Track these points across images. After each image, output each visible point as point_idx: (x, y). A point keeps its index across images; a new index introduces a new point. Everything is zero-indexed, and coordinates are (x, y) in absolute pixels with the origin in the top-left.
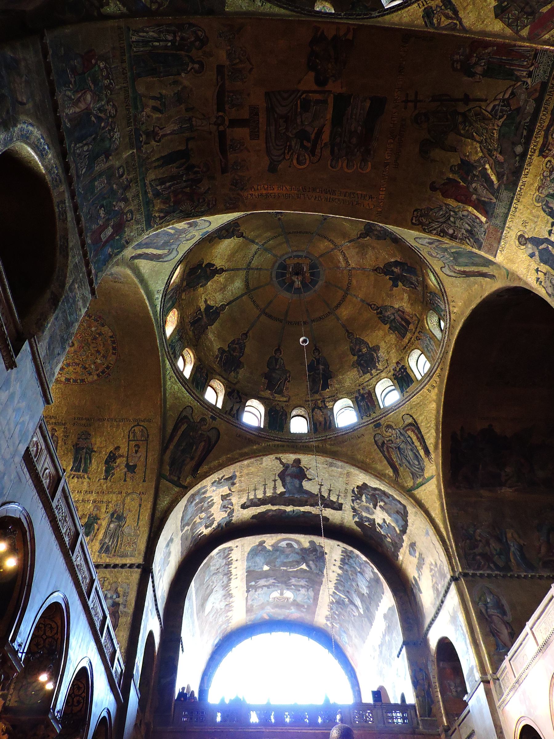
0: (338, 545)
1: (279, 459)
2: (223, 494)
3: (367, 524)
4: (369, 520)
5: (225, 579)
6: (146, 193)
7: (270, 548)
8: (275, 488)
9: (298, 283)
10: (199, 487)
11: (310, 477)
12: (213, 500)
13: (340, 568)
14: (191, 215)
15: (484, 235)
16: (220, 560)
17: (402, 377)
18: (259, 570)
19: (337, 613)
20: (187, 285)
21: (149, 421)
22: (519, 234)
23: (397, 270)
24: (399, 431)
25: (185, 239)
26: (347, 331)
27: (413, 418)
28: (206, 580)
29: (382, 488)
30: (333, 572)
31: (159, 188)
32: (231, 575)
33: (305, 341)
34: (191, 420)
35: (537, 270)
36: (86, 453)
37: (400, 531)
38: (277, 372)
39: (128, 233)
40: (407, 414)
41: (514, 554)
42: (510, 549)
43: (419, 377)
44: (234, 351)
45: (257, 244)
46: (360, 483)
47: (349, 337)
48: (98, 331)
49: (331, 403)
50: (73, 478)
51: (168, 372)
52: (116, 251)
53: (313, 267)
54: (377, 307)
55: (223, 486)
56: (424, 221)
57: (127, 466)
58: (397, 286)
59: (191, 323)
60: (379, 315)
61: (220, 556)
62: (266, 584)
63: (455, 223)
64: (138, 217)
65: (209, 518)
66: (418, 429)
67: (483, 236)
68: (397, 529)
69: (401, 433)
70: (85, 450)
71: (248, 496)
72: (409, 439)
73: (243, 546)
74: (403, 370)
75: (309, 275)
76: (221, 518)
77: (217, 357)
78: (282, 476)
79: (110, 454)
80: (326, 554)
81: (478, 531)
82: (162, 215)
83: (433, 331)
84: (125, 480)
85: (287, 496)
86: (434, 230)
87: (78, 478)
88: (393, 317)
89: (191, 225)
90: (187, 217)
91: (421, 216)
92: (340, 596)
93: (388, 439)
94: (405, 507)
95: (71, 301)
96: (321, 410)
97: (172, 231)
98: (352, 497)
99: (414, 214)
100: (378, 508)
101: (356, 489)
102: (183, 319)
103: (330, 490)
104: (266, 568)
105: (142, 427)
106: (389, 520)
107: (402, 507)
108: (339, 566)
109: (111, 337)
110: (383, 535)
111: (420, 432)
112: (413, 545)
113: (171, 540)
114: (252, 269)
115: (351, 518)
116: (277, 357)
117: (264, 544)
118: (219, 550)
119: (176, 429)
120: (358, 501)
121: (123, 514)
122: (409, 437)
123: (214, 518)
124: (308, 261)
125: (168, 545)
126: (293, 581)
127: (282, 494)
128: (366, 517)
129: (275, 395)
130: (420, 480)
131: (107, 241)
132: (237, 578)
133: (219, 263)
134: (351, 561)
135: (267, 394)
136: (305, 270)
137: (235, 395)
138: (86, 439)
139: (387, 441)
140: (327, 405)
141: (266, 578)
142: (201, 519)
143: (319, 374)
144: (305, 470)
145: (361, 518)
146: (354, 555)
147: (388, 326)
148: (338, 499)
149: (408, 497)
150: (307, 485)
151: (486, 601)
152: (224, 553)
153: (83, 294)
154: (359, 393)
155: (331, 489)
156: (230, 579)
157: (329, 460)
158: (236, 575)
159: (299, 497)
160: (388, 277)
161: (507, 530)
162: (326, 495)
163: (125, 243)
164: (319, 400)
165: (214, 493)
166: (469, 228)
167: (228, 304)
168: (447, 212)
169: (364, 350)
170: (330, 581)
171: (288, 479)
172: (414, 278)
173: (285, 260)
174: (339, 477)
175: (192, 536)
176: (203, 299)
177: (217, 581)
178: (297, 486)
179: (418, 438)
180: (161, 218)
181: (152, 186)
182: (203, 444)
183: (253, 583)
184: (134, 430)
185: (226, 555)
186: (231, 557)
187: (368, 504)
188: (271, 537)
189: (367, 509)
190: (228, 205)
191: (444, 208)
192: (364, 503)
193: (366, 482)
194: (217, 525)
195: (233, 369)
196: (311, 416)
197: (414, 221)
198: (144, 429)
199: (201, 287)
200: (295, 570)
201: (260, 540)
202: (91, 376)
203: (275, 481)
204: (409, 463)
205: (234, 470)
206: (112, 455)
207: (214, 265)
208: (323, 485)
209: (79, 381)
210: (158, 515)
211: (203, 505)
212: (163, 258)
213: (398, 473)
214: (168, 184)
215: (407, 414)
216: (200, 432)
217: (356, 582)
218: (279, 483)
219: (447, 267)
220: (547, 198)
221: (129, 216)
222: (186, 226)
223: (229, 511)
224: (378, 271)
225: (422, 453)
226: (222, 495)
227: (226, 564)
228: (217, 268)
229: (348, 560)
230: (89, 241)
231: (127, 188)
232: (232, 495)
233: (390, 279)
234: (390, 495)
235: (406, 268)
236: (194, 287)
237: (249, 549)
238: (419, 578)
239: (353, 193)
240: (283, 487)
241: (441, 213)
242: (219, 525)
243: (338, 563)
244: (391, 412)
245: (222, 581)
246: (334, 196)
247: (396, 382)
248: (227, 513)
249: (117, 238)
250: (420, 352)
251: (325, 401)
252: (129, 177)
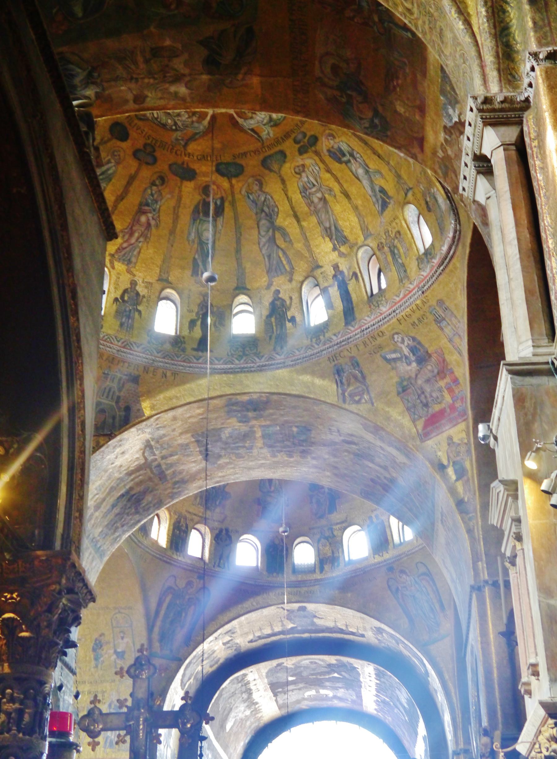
5: (245, 696)
21: (130, 608)
33: (284, 532)
57: (116, 652)
66: (433, 580)
72: (424, 589)
111: (435, 584)
215: (421, 563)
216: (187, 597)
225: (437, 606)
237: (266, 671)
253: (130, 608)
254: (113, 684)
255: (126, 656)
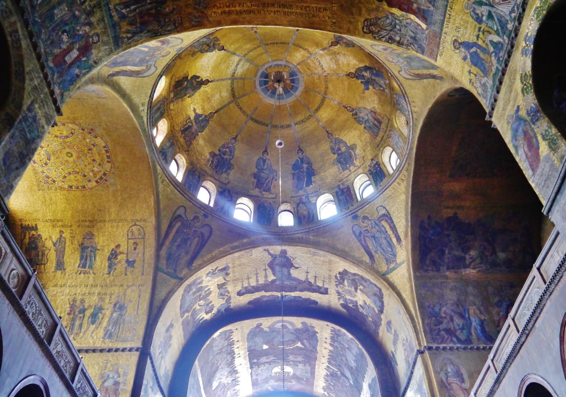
0: (327, 325)
1: (267, 251)
2: (219, 283)
3: (351, 305)
4: (352, 302)
5: (229, 358)
6: (111, 16)
7: (267, 330)
8: (266, 276)
9: (280, 90)
10: (194, 278)
11: (296, 266)
12: (209, 289)
13: (331, 345)
14: (159, 34)
15: (426, 41)
16: (223, 342)
17: (376, 172)
18: (260, 349)
19: (332, 384)
20: (174, 97)
21: (145, 221)
22: (454, 39)
23: (367, 74)
24: (375, 221)
25: (160, 56)
26: (327, 132)
27: (386, 210)
28: (210, 359)
29: (360, 273)
30: (325, 348)
31: (124, 11)
32: (235, 354)
33: (280, 144)
34: (186, 219)
35: (470, 72)
36: (91, 251)
37: (378, 311)
38: (265, 171)
39: (95, 54)
40: (381, 206)
41: (476, 329)
42: (471, 324)
43: (391, 172)
44: (224, 154)
45: (239, 56)
46: (341, 270)
47: (329, 137)
48: (92, 142)
49: (315, 198)
50: (80, 274)
51: (160, 176)
52: (84, 71)
53: (292, 74)
54: (352, 109)
55: (218, 276)
56: (374, 29)
57: (127, 261)
58: (368, 89)
59: (181, 131)
60: (355, 117)
61: (222, 338)
62: (267, 361)
63: (400, 30)
64: (105, 39)
65: (208, 305)
66: (391, 219)
67: (425, 41)
68: (376, 309)
69: (375, 223)
70: (89, 249)
71: (243, 284)
72: (383, 229)
73: (242, 328)
74: (377, 166)
75: (289, 82)
76: (219, 305)
77: (208, 161)
78: (271, 266)
79: (112, 252)
80: (317, 333)
81: (444, 309)
82: (129, 35)
83: (401, 129)
84: (126, 275)
85: (278, 283)
86: (383, 37)
87: (84, 273)
88: (366, 118)
89: (163, 42)
90: (155, 36)
91: (371, 25)
92: (333, 370)
93: (364, 229)
94: (380, 290)
95: (30, 120)
96: (305, 205)
97: (146, 50)
98: (336, 282)
99: (364, 24)
100: (359, 291)
101: (338, 275)
102: (174, 128)
103: (316, 277)
104: (265, 347)
105: (139, 227)
106: (368, 301)
107: (378, 289)
108: (330, 344)
109: (105, 147)
110: (365, 315)
112: (389, 323)
113: (171, 326)
114: (236, 79)
115: (337, 300)
116: (264, 158)
117: (261, 327)
118: (220, 333)
119: (170, 227)
120: (341, 285)
121: (124, 304)
122: (383, 226)
123: (213, 305)
124: (287, 70)
125: (168, 330)
126: (291, 358)
127: (273, 281)
128: (349, 299)
129: (264, 193)
130: (392, 266)
131: (73, 63)
132: (240, 356)
133: (204, 75)
134: (339, 338)
135: (256, 192)
136: (285, 78)
137: (226, 193)
138: (90, 239)
139: (364, 231)
140: (311, 199)
141: (267, 356)
142: (200, 306)
143: (303, 172)
144: (292, 259)
145: (345, 300)
146: (341, 333)
147: (363, 126)
148: (323, 284)
149: (383, 281)
150: (294, 273)
151: (447, 370)
152: (225, 335)
153: (46, 113)
154: (339, 188)
155: (317, 275)
156: (234, 358)
157: (313, 250)
158: (239, 354)
159: (288, 283)
160: (360, 81)
161: (470, 307)
162: (312, 281)
163: (93, 64)
164: (303, 195)
165: (210, 283)
166: (413, 35)
167: (216, 112)
168: (393, 21)
169: (343, 149)
170: (324, 357)
171: (277, 269)
172: (382, 82)
173: (266, 69)
174: (323, 265)
175: (194, 321)
176: (192, 109)
177: (221, 359)
178: (286, 273)
179: (391, 227)
180: (129, 38)
181: (117, 10)
182: (197, 239)
183: (255, 361)
184: (132, 229)
185: (227, 337)
186: (232, 338)
187: (350, 288)
188: (267, 319)
189: (350, 292)
190: (194, 23)
191: (390, 17)
192: (347, 288)
193: (346, 269)
194: (216, 310)
195: (224, 171)
196: (296, 211)
197: (365, 30)
198: (141, 229)
199: (189, 97)
200: (292, 348)
201: (257, 323)
202: (91, 183)
203: (265, 270)
204: (384, 250)
205: (226, 262)
206: (113, 252)
207: (199, 77)
208: (308, 272)
209: (80, 188)
210: (157, 303)
211: (201, 294)
212: (142, 74)
213: (374, 259)
214: (132, 7)
215: (381, 206)
216: (194, 229)
217: (346, 357)
218: (269, 272)
219: (403, 70)
220: (474, 6)
221: (95, 39)
222: (159, 44)
223: (227, 298)
224: (351, 76)
225: (394, 240)
226: (218, 285)
227: (228, 345)
228: (202, 79)
229: (337, 337)
230: (51, 65)
231: (90, 14)
232: (227, 284)
233: (362, 82)
234: (367, 279)
235: (375, 72)
236: (182, 98)
237: (248, 331)
238: (395, 351)
239: (309, 7)
240: (273, 276)
241: (388, 21)
242: (219, 311)
243: (329, 341)
244: (367, 205)
245: (226, 360)
246: (291, 10)
247: (371, 176)
248: (225, 300)
249: (84, 59)
250: (392, 149)
251: (308, 197)
252: (92, 4)
253: (145, 221)
254: (121, 288)
255: (135, 265)
